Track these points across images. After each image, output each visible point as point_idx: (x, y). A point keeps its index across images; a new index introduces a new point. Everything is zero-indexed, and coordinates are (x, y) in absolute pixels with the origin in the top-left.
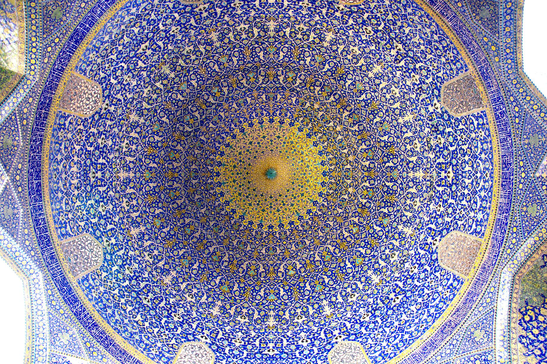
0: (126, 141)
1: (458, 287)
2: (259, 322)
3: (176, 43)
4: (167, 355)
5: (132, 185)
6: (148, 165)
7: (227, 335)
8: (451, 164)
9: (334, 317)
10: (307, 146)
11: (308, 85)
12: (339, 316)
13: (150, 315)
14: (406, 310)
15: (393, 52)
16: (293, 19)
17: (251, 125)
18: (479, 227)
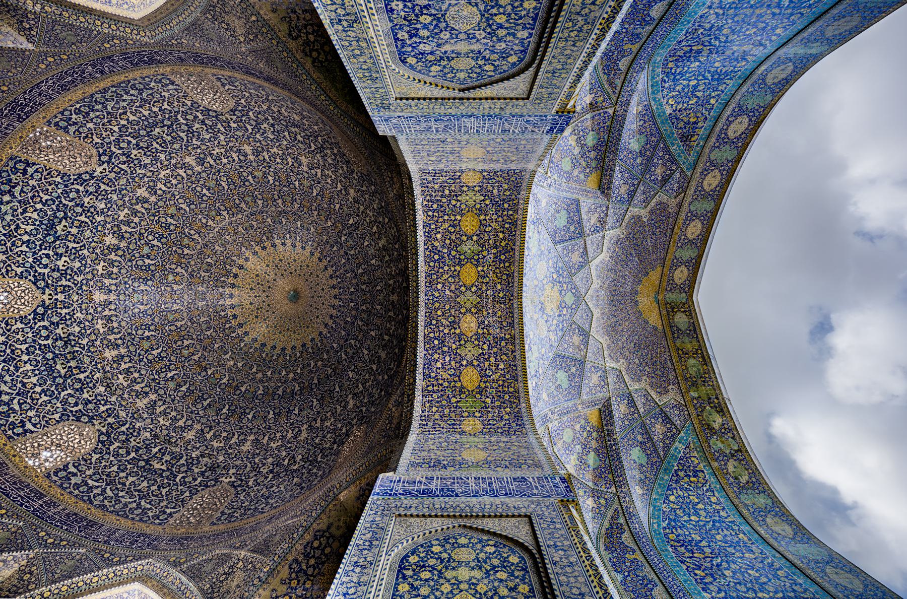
0: (334, 177)
2: (116, 229)
14: (37, 372)
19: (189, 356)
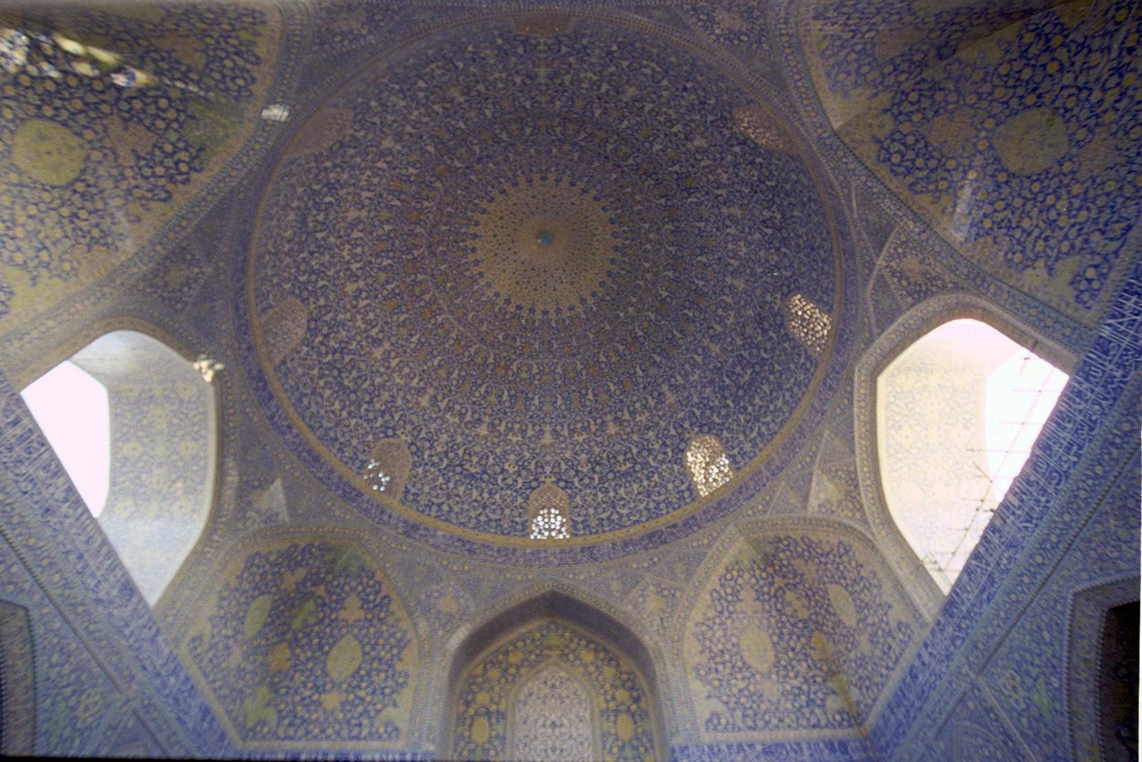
5: (360, 227)
11: (641, 172)
15: (766, 213)
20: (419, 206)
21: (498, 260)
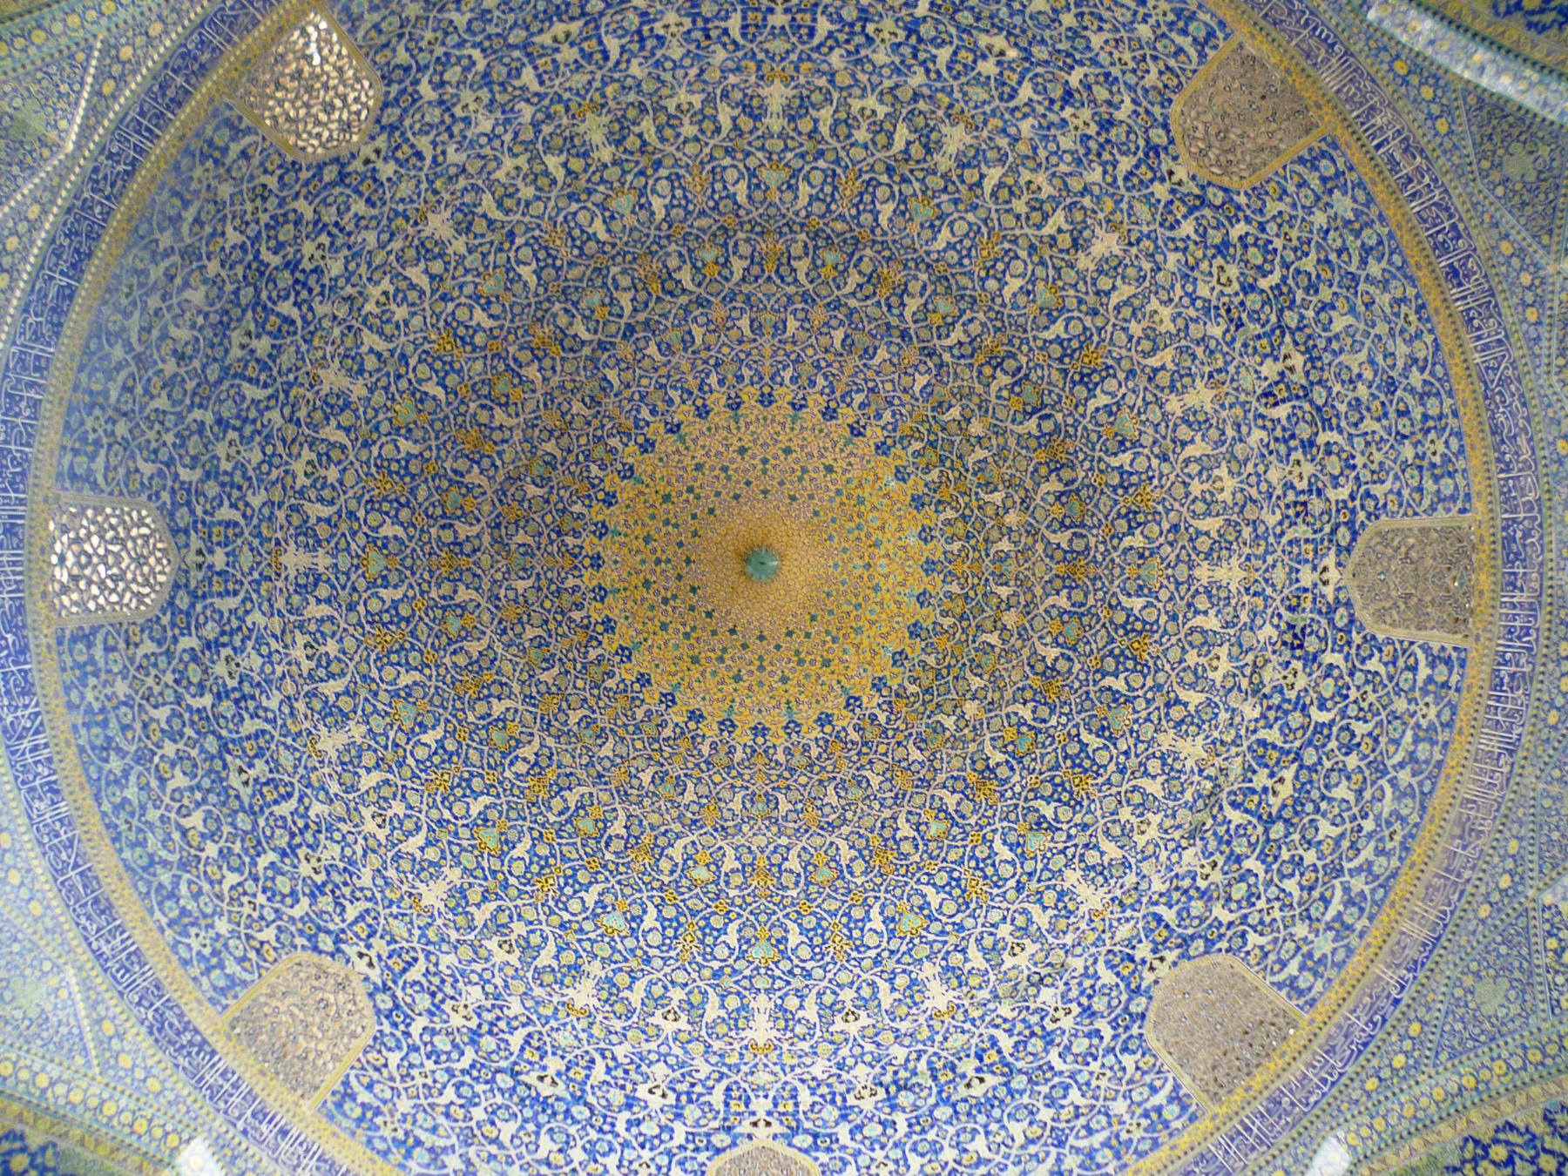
0: (386, 284)
1: (1177, 1124)
2: (548, 978)
3: (657, 64)
4: (232, 967)
5: (346, 418)
6: (420, 382)
7: (436, 981)
8: (1298, 757)
9: (773, 1056)
10: (900, 529)
11: (980, 358)
12: (788, 1060)
13: (233, 825)
14: (994, 1127)
15: (1270, 369)
16: (1023, 148)
17: (766, 400)
18: (1308, 975)
19: (949, 816)
20: (483, 417)
21: (650, 596)
